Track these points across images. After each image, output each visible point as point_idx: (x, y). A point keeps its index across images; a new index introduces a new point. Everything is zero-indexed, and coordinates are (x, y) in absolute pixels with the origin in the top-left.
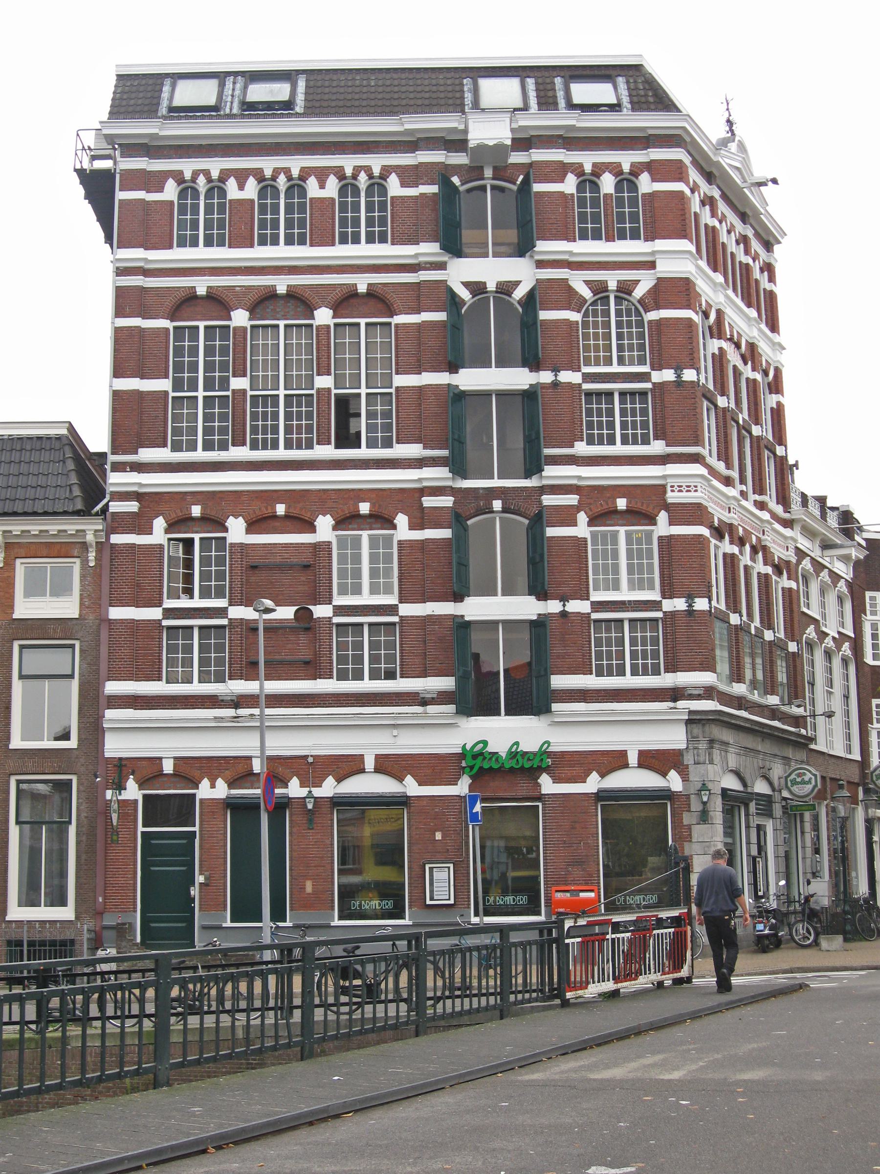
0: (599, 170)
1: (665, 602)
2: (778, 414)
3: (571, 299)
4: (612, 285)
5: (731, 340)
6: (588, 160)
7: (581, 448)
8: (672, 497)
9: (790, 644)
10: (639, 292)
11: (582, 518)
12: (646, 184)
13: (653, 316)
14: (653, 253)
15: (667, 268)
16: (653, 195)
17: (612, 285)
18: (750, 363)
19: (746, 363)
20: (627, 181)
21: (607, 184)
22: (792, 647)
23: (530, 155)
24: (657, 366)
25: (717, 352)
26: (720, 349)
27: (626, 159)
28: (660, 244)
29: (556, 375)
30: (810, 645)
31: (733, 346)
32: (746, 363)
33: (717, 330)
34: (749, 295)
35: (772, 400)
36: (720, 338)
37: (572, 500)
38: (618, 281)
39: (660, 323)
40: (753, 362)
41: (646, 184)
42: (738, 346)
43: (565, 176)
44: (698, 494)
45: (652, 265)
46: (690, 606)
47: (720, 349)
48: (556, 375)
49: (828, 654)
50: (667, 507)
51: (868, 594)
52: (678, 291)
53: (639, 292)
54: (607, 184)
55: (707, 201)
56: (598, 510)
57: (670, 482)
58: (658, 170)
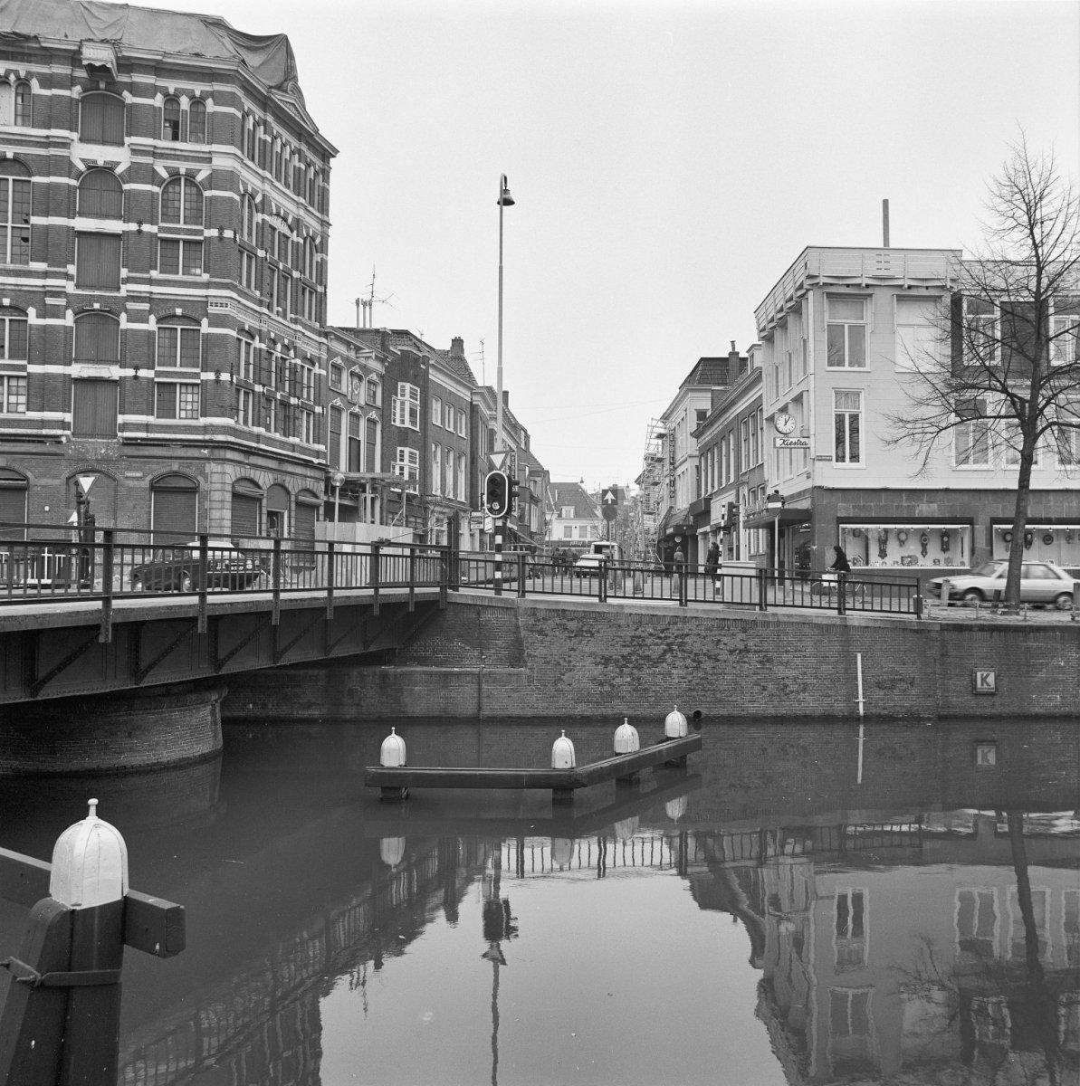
0: (179, 93)
1: (29, 366)
2: (322, 266)
3: (153, 177)
4: (183, 171)
5: (278, 215)
6: (172, 85)
7: (155, 274)
8: (211, 310)
9: (317, 407)
10: (200, 178)
11: (152, 318)
12: (211, 106)
13: (207, 193)
14: (210, 152)
15: (219, 162)
16: (214, 114)
17: (183, 171)
18: (295, 232)
19: (292, 231)
20: (197, 102)
21: (185, 103)
22: (318, 409)
23: (131, 77)
24: (208, 227)
25: (260, 221)
26: (263, 220)
27: (198, 88)
28: (215, 147)
29: (140, 226)
30: (337, 410)
31: (280, 220)
32: (292, 231)
33: (264, 207)
34: (299, 189)
35: (318, 257)
36: (263, 213)
37: (146, 306)
38: (15, 153)
39: (211, 199)
40: (298, 231)
41: (211, 106)
42: (285, 219)
43: (155, 94)
44: (228, 309)
45: (209, 160)
46: (218, 377)
47: (263, 220)
48: (140, 226)
49: (355, 416)
50: (126, 311)
51: (400, 384)
52: (229, 179)
53: (200, 178)
54: (185, 103)
55: (261, 122)
56: (162, 313)
57: (210, 300)
58: (219, 98)
